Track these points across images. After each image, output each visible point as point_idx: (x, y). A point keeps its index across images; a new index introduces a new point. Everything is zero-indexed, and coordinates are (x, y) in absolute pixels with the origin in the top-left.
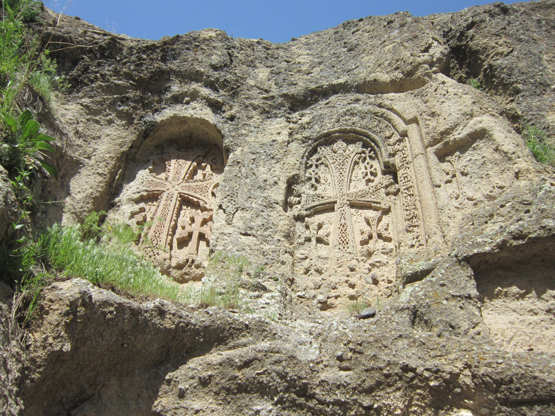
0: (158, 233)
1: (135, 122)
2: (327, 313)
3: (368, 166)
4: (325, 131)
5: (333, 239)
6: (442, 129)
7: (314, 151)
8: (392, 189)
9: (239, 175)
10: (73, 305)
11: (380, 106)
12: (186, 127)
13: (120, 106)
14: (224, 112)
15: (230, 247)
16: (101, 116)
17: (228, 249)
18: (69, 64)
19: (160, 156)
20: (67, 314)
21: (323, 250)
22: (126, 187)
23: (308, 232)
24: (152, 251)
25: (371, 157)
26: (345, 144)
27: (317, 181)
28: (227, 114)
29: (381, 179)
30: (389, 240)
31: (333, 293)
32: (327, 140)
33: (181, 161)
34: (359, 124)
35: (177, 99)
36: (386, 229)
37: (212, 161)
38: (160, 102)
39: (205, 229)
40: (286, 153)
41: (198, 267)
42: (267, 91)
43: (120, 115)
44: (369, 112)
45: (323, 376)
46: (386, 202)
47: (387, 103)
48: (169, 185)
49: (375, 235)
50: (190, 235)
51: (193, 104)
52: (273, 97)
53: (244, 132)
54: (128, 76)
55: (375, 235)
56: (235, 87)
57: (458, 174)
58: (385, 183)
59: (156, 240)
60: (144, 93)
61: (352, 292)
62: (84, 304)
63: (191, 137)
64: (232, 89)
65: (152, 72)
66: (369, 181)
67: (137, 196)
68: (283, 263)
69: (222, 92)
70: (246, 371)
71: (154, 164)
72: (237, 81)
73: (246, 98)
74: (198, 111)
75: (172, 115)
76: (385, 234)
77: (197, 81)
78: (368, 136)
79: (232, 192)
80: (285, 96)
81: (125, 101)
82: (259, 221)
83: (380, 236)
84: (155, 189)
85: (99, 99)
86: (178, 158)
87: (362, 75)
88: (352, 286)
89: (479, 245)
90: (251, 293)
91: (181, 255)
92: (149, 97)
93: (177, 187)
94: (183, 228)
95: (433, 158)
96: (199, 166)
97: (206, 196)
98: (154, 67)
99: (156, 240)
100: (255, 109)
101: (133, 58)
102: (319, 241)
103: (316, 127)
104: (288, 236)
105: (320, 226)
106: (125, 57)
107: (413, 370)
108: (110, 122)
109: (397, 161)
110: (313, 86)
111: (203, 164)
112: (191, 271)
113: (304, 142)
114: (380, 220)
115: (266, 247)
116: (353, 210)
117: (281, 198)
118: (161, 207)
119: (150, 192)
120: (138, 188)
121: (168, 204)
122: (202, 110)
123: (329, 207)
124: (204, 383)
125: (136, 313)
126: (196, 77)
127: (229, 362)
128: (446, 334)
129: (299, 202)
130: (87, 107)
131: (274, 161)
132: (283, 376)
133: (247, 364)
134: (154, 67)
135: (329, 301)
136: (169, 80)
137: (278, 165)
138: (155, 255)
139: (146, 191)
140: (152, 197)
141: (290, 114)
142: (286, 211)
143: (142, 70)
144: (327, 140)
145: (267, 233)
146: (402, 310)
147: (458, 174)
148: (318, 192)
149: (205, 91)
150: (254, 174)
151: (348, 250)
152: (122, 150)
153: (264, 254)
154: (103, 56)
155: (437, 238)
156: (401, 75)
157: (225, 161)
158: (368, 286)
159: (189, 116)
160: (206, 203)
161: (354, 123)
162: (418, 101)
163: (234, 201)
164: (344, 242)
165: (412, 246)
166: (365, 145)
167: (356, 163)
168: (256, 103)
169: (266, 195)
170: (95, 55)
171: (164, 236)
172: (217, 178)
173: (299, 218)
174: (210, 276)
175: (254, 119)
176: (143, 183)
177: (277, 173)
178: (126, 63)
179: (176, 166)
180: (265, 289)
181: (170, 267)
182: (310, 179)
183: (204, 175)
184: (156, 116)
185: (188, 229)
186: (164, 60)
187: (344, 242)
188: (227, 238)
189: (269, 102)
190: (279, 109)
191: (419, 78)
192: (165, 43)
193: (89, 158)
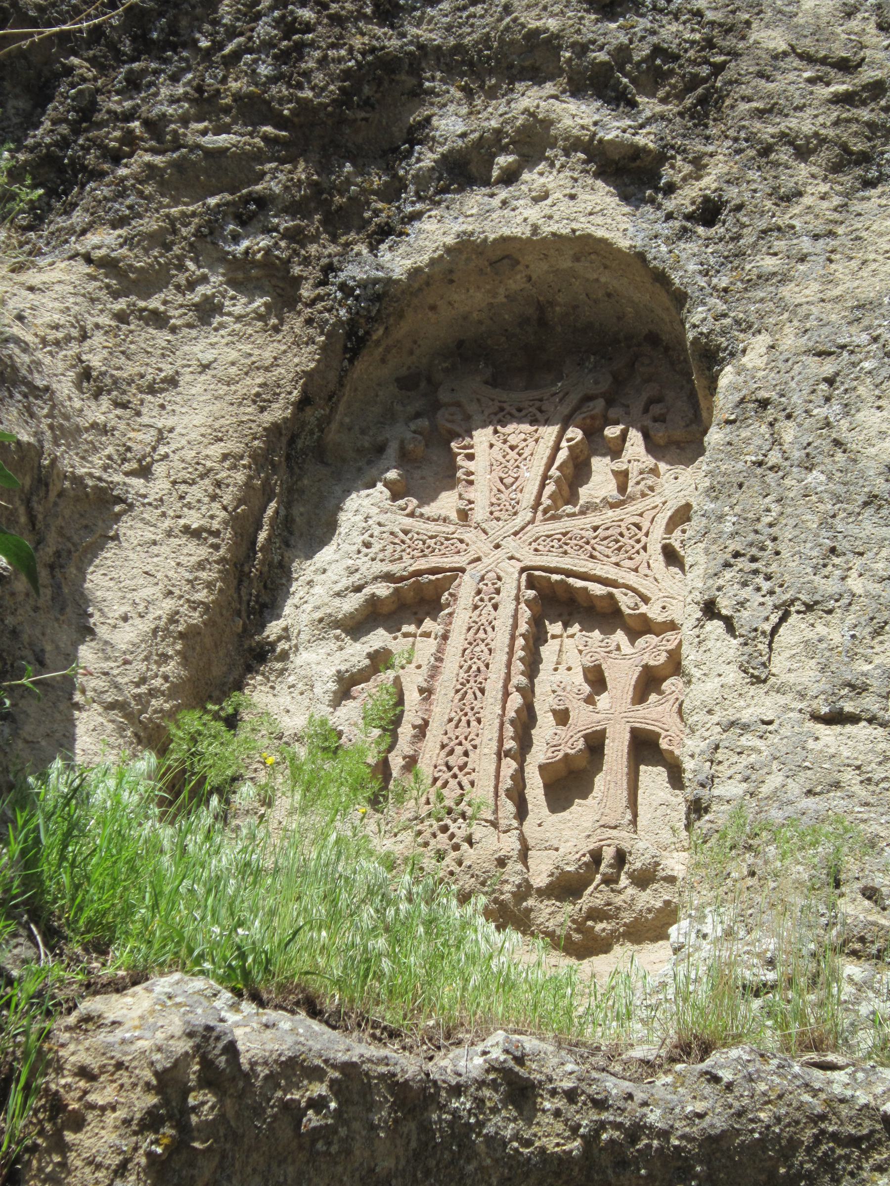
0: (459, 750)
1: (306, 292)
9: (774, 458)
10: (168, 1083)
12: (516, 283)
13: (236, 238)
14: (670, 189)
15: (774, 781)
16: (169, 293)
17: (765, 790)
18: (21, 104)
19: (424, 423)
20: (151, 1122)
22: (305, 570)
24: (445, 829)
28: (686, 198)
33: (516, 431)
35: (464, 171)
37: (646, 410)
39: (656, 714)
41: (643, 879)
42: (845, 66)
43: (240, 276)
48: (478, 543)
50: (595, 745)
51: (533, 178)
53: (769, 263)
54: (253, 109)
56: (705, 71)
59: (453, 783)
60: (324, 168)
62: (211, 1078)
63: (542, 322)
64: (694, 82)
65: (347, 74)
67: (352, 603)
69: (649, 106)
71: (405, 459)
72: (709, 43)
73: (760, 114)
75: (450, 240)
77: (537, 77)
79: (752, 537)
81: (251, 213)
84: (422, 564)
85: (150, 224)
86: (500, 417)
91: (564, 836)
92: (348, 182)
93: (510, 545)
94: (562, 717)
96: (595, 442)
97: (643, 570)
98: (351, 50)
99: (453, 783)
100: (803, 153)
101: (264, 29)
106: (232, 33)
108: (207, 311)
111: (613, 432)
112: (618, 900)
118: (457, 640)
119: (402, 579)
120: (352, 571)
121: (483, 620)
122: (572, 197)
125: (416, 1099)
126: (530, 58)
130: (109, 265)
134: (351, 50)
136: (418, 94)
138: (456, 847)
139: (388, 577)
140: (416, 600)
143: (307, 74)
149: (577, 115)
150: (837, 443)
152: (268, 418)
154: (145, 46)
157: (703, 404)
159: (522, 231)
160: (646, 600)
163: (768, 578)
168: (807, 128)
170: (113, 47)
171: (484, 762)
172: (680, 484)
174: (702, 918)
175: (807, 200)
176: (368, 545)
178: (236, 56)
179: (496, 453)
181: (524, 890)
183: (622, 477)
184: (385, 255)
185: (583, 718)
188: (758, 743)
189: (865, 114)
193: (144, 472)
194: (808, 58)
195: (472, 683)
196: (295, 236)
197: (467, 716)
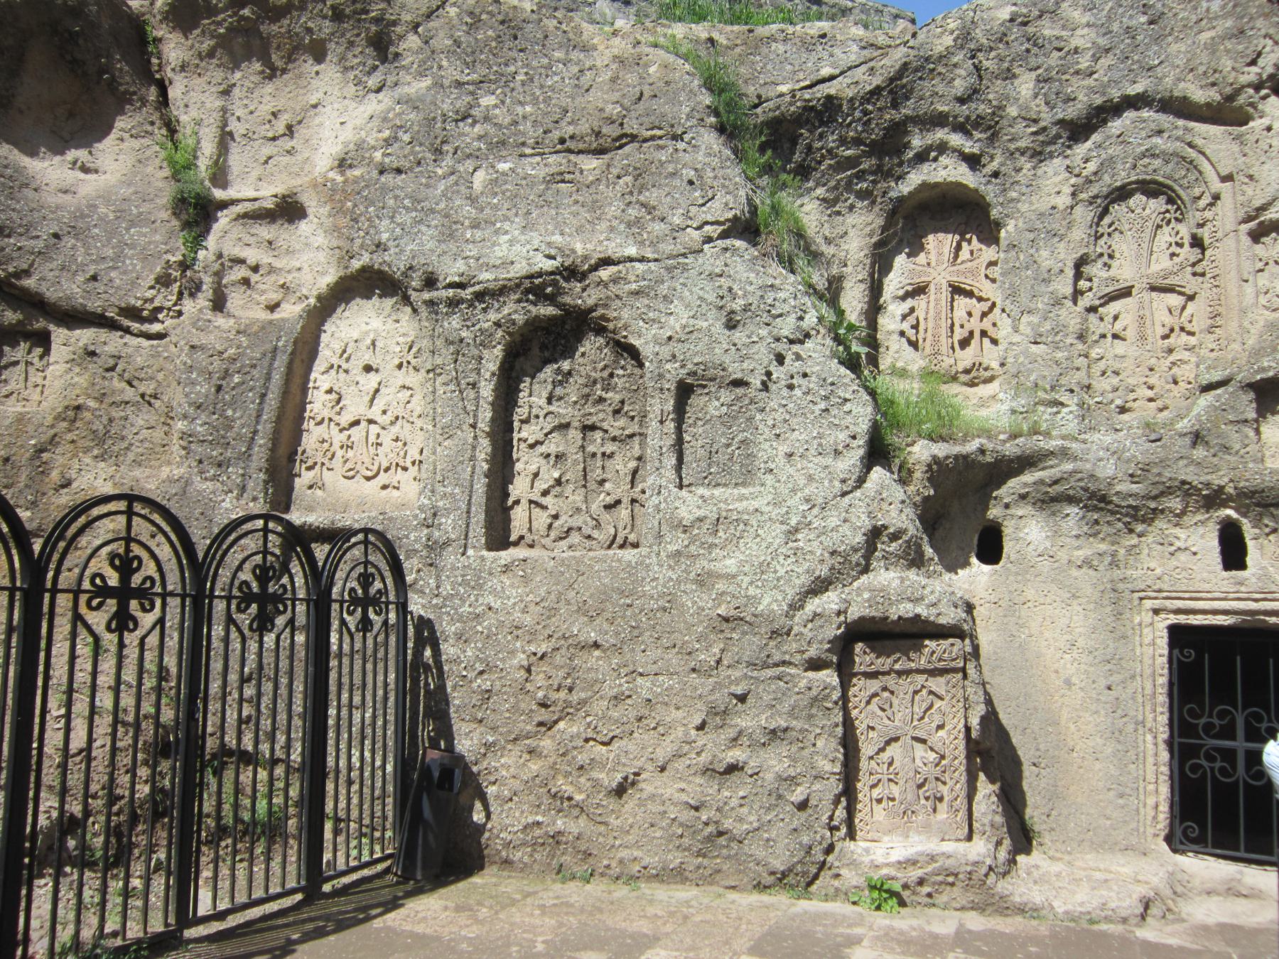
1: (879, 200)
2: (1125, 417)
3: (1173, 233)
4: (1118, 184)
5: (1130, 334)
6: (1257, 203)
7: (1106, 211)
8: (1198, 269)
10: (929, 466)
11: (1190, 145)
14: (984, 166)
15: (1021, 359)
16: (840, 204)
20: (927, 472)
21: (1119, 348)
22: (886, 281)
23: (1102, 324)
25: (1176, 219)
26: (1144, 198)
27: (1111, 257)
28: (989, 169)
29: (1188, 253)
30: (1191, 334)
31: (1132, 396)
32: (1122, 194)
33: (941, 236)
34: (1159, 170)
35: (922, 157)
36: (1190, 322)
38: (901, 164)
39: (986, 324)
40: (1070, 226)
41: (986, 369)
42: (1035, 121)
44: (1175, 154)
45: (1118, 488)
46: (1191, 285)
47: (1199, 142)
49: (1177, 329)
50: (971, 333)
51: (943, 160)
52: (1044, 129)
53: (1014, 195)
54: (857, 142)
55: (1177, 329)
57: (1271, 262)
58: (1193, 259)
60: (880, 159)
61: (1150, 394)
62: (936, 463)
64: (990, 127)
66: (1173, 255)
67: (901, 293)
68: (1078, 369)
69: (977, 135)
70: (1055, 487)
71: (909, 245)
72: (994, 113)
73: (1010, 140)
74: (948, 171)
76: (1188, 327)
77: (942, 125)
78: (1174, 191)
80: (1061, 122)
81: (860, 176)
82: (1048, 326)
83: (1182, 329)
85: (833, 183)
86: (935, 231)
87: (1168, 81)
88: (1151, 388)
89: (1264, 370)
90: (1049, 410)
91: (966, 358)
94: (962, 326)
95: (1246, 240)
96: (963, 239)
100: (1022, 154)
101: (857, 114)
102: (1115, 336)
103: (1106, 178)
104: (1081, 337)
105: (1116, 318)
106: (848, 115)
107: (1190, 483)
108: (852, 207)
109: (1205, 233)
110: (1099, 101)
111: (968, 236)
113: (1091, 203)
114: (1184, 308)
115: (1059, 355)
116: (1154, 294)
117: (1069, 290)
118: (932, 304)
121: (938, 296)
123: (1126, 293)
124: (1023, 497)
125: (965, 457)
126: (940, 120)
127: (1042, 482)
128: (1220, 454)
129: (1091, 289)
130: (824, 200)
131: (1056, 239)
132: (1086, 490)
133: (1056, 482)
135: (1127, 405)
136: (906, 133)
137: (1062, 245)
140: (919, 290)
141: (1069, 147)
142: (1075, 303)
144: (1122, 194)
145: (1058, 338)
146: (1185, 434)
147: (1271, 262)
148: (1112, 272)
149: (956, 140)
151: (1148, 348)
152: (873, 240)
153: (1057, 363)
154: (822, 124)
155: (1236, 346)
156: (1218, 98)
158: (1168, 387)
161: (1155, 171)
162: (1235, 148)
164: (1143, 338)
165: (1212, 350)
166: (1170, 201)
167: (1159, 227)
168: (1024, 145)
169: (1050, 289)
170: (813, 124)
171: (943, 339)
172: (989, 253)
173: (1092, 309)
175: (1024, 171)
177: (1062, 256)
178: (850, 124)
180: (1062, 404)
181: (957, 372)
182: (1101, 255)
183: (972, 252)
185: (968, 327)
186: (895, 105)
187: (1143, 338)
190: (1055, 143)
191: (1241, 107)
192: (892, 80)
193: (846, 265)
194: (1024, 119)
195: (937, 317)
196: (874, 182)
197: (937, 327)
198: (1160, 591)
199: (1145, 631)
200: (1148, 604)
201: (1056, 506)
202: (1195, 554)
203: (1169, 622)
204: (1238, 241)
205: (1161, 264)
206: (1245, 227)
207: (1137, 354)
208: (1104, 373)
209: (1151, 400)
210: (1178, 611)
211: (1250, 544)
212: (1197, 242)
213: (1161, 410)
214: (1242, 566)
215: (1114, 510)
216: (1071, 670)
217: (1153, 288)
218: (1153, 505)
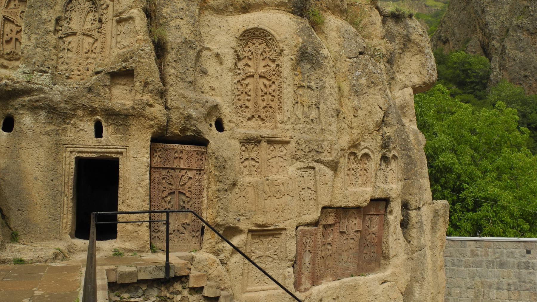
2: (69, 81)
5: (74, 50)
6: (120, 11)
8: (100, 30)
15: (30, 52)
21: (70, 55)
29: (97, 23)
30: (95, 53)
45: (61, 105)
46: (97, 36)
49: (90, 51)
50: (11, 39)
55: (90, 51)
58: (98, 27)
61: (79, 73)
66: (92, 23)
68: (53, 60)
70: (37, 103)
76: (94, 51)
83: (92, 51)
88: (79, 71)
89: (114, 68)
90: (39, 74)
94: (8, 35)
95: (115, 23)
104: (55, 47)
105: (70, 43)
109: (103, 18)
114: (94, 44)
116: (84, 37)
117: (52, 29)
123: (74, 34)
124: (24, 106)
127: (31, 100)
132: (48, 105)
133: (37, 101)
135: (70, 76)
137: (51, 11)
145: (46, 47)
158: (85, 71)
164: (78, 52)
166: (93, 4)
167: (89, 12)
169: (45, 27)
172: (22, 8)
173: (61, 38)
177: (51, 15)
181: (3, 54)
182: (67, 18)
185: (10, 36)
187: (78, 52)
198: (73, 145)
199: (67, 159)
200: (69, 149)
201: (37, 111)
202: (86, 131)
203: (76, 156)
204: (112, 23)
205: (88, 26)
206: (115, 19)
207: (75, 58)
208: (63, 63)
209: (79, 75)
210: (79, 152)
211: (104, 128)
212: (100, 21)
213: (82, 80)
214: (101, 137)
215: (58, 114)
216: (37, 174)
217: (84, 34)
218: (73, 113)
